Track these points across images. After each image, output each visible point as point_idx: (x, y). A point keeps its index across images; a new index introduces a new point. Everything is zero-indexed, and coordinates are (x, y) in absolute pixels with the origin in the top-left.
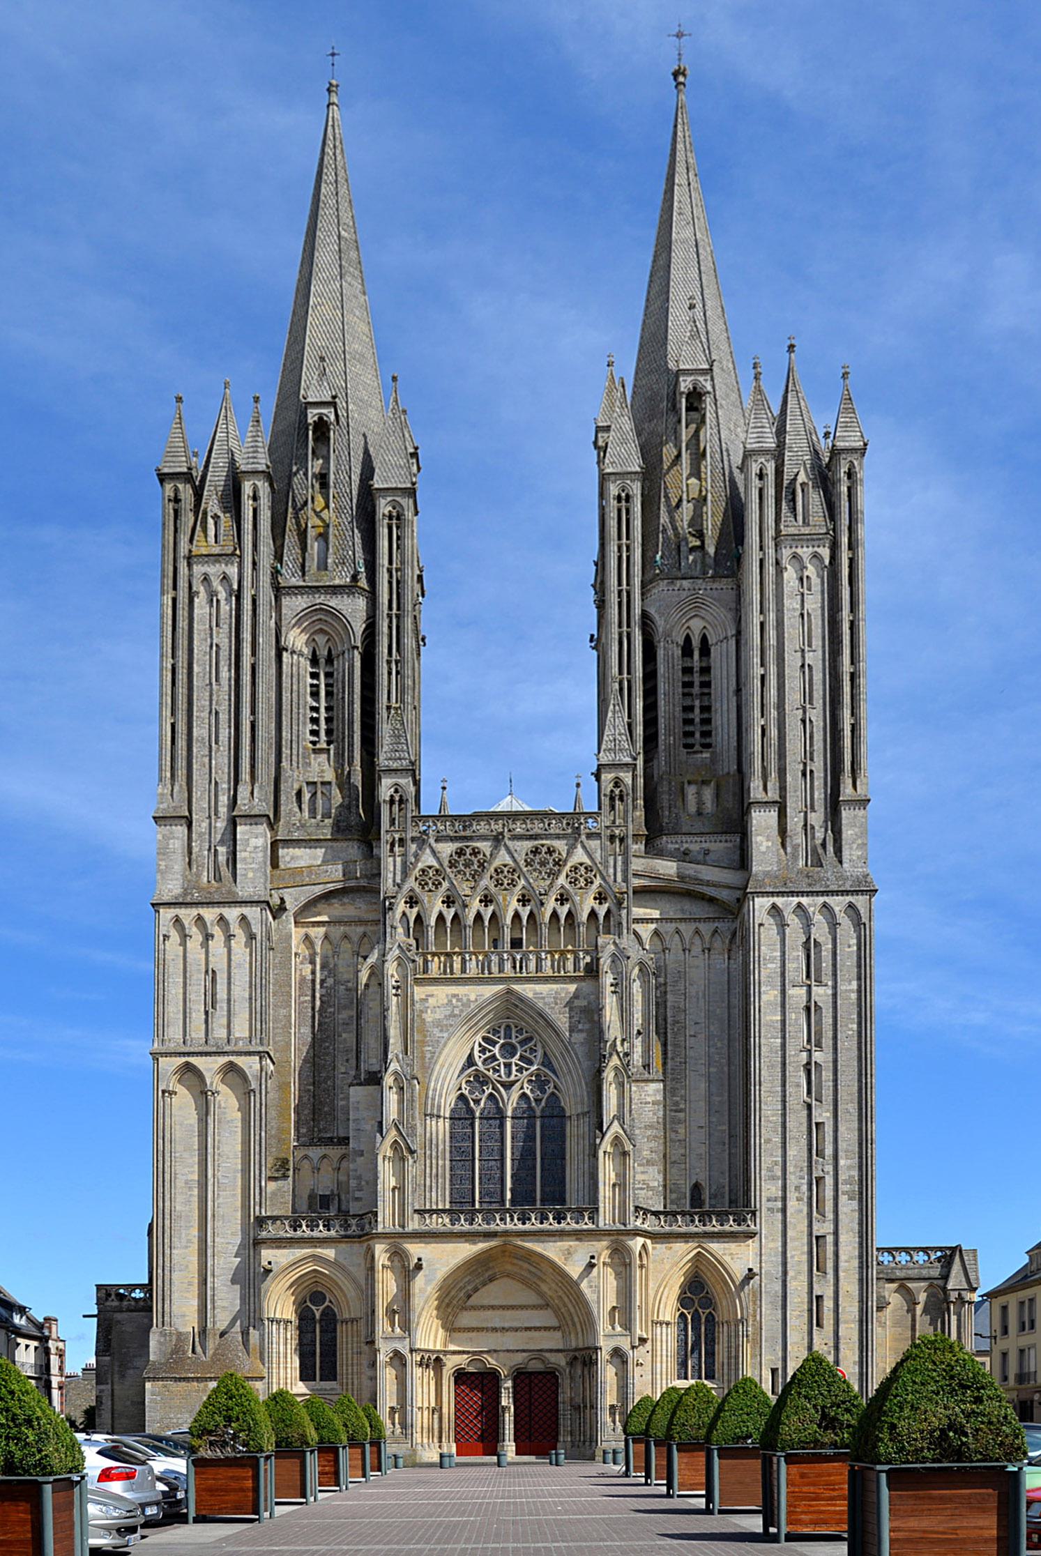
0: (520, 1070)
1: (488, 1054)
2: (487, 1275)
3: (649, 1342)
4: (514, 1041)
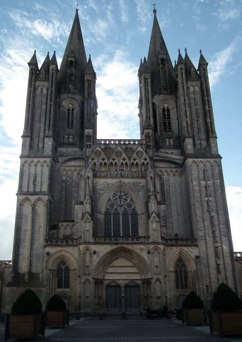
0: (124, 202)
3: (168, 277)
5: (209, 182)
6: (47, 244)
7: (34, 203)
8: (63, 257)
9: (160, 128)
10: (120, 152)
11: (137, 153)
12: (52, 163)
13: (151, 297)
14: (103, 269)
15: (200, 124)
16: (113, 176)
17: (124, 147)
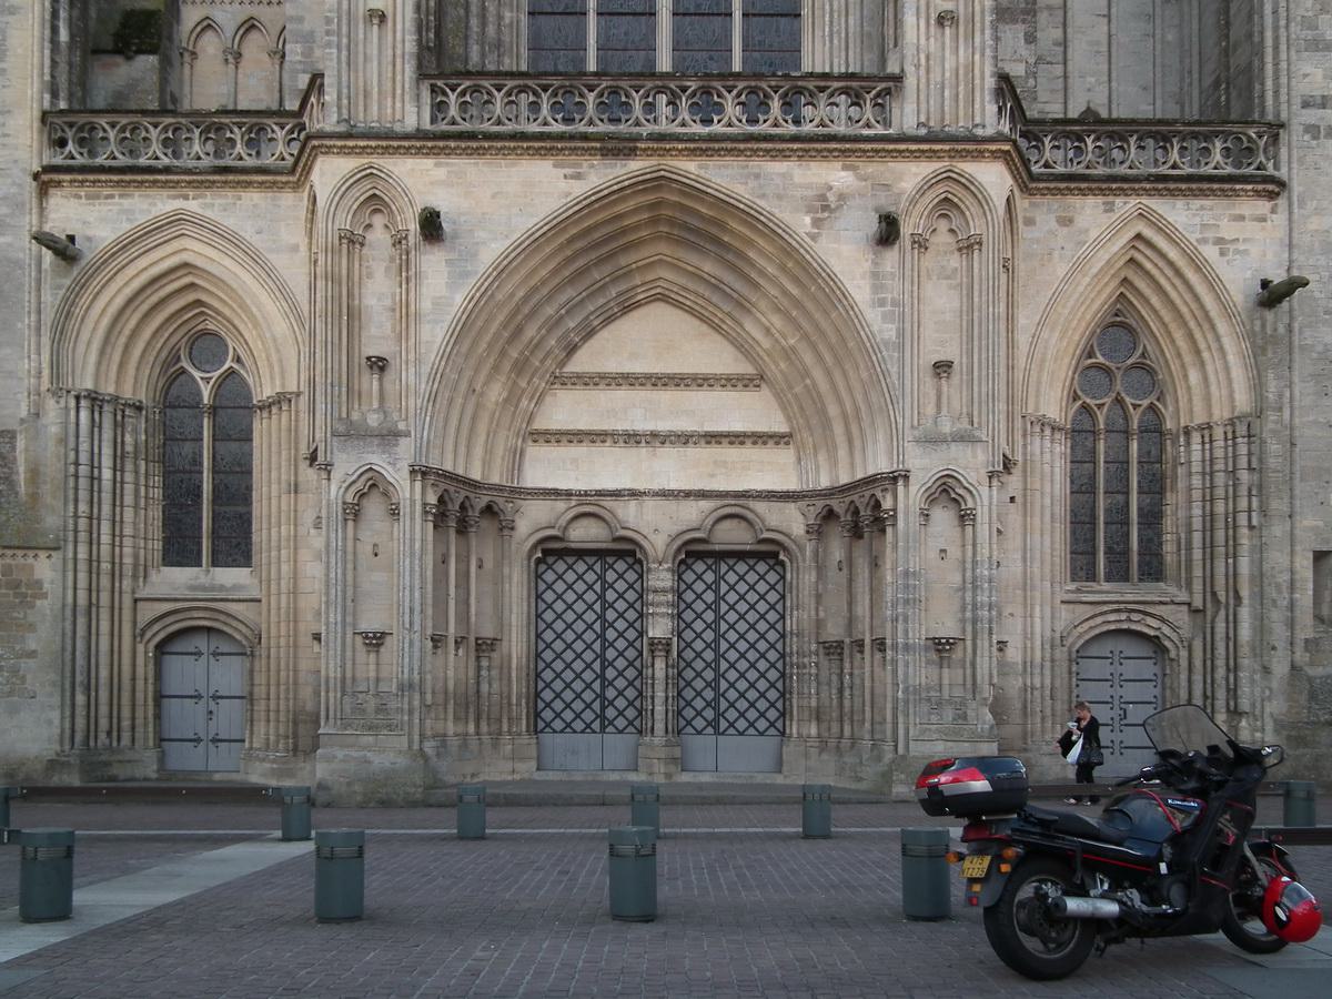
3: (1017, 471)
14: (512, 399)
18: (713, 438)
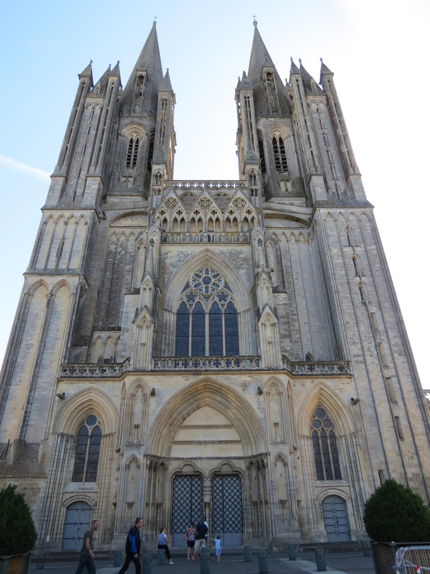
1: (197, 282)
2: (195, 404)
4: (210, 275)
5: (358, 249)
6: (64, 375)
7: (52, 291)
8: (91, 404)
9: (270, 166)
10: (207, 201)
11: (235, 201)
12: (94, 219)
13: (266, 502)
14: (169, 433)
15: (331, 156)
16: (195, 240)
17: (214, 192)
18: (220, 442)
